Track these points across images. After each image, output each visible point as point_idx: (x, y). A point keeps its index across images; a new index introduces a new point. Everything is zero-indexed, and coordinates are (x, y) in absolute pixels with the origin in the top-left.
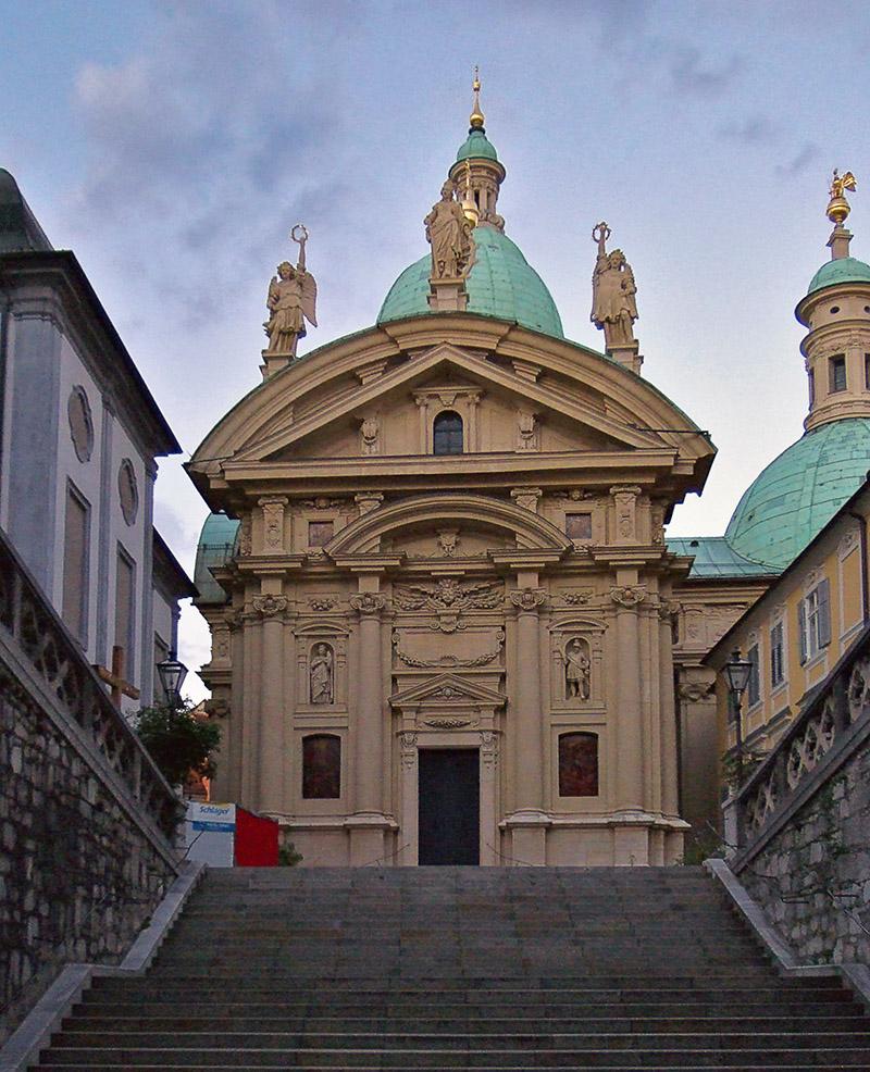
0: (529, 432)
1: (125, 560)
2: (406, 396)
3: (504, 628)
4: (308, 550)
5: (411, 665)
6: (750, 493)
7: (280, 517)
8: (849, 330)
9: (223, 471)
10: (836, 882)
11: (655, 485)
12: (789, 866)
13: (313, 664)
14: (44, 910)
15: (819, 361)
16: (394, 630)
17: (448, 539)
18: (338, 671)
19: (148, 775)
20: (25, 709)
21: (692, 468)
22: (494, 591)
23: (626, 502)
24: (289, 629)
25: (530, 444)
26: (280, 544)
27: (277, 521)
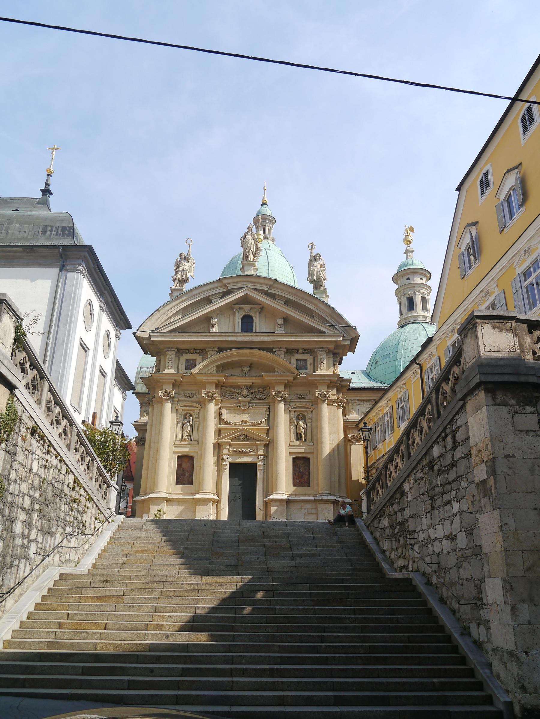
0: (281, 324)
1: (103, 374)
2: (231, 307)
3: (269, 408)
5: (227, 424)
6: (376, 353)
8: (414, 287)
9: (150, 337)
10: (408, 531)
12: (389, 523)
14: (40, 539)
15: (402, 298)
19: (100, 474)
20: (42, 442)
22: (265, 392)
23: (322, 355)
25: (282, 329)
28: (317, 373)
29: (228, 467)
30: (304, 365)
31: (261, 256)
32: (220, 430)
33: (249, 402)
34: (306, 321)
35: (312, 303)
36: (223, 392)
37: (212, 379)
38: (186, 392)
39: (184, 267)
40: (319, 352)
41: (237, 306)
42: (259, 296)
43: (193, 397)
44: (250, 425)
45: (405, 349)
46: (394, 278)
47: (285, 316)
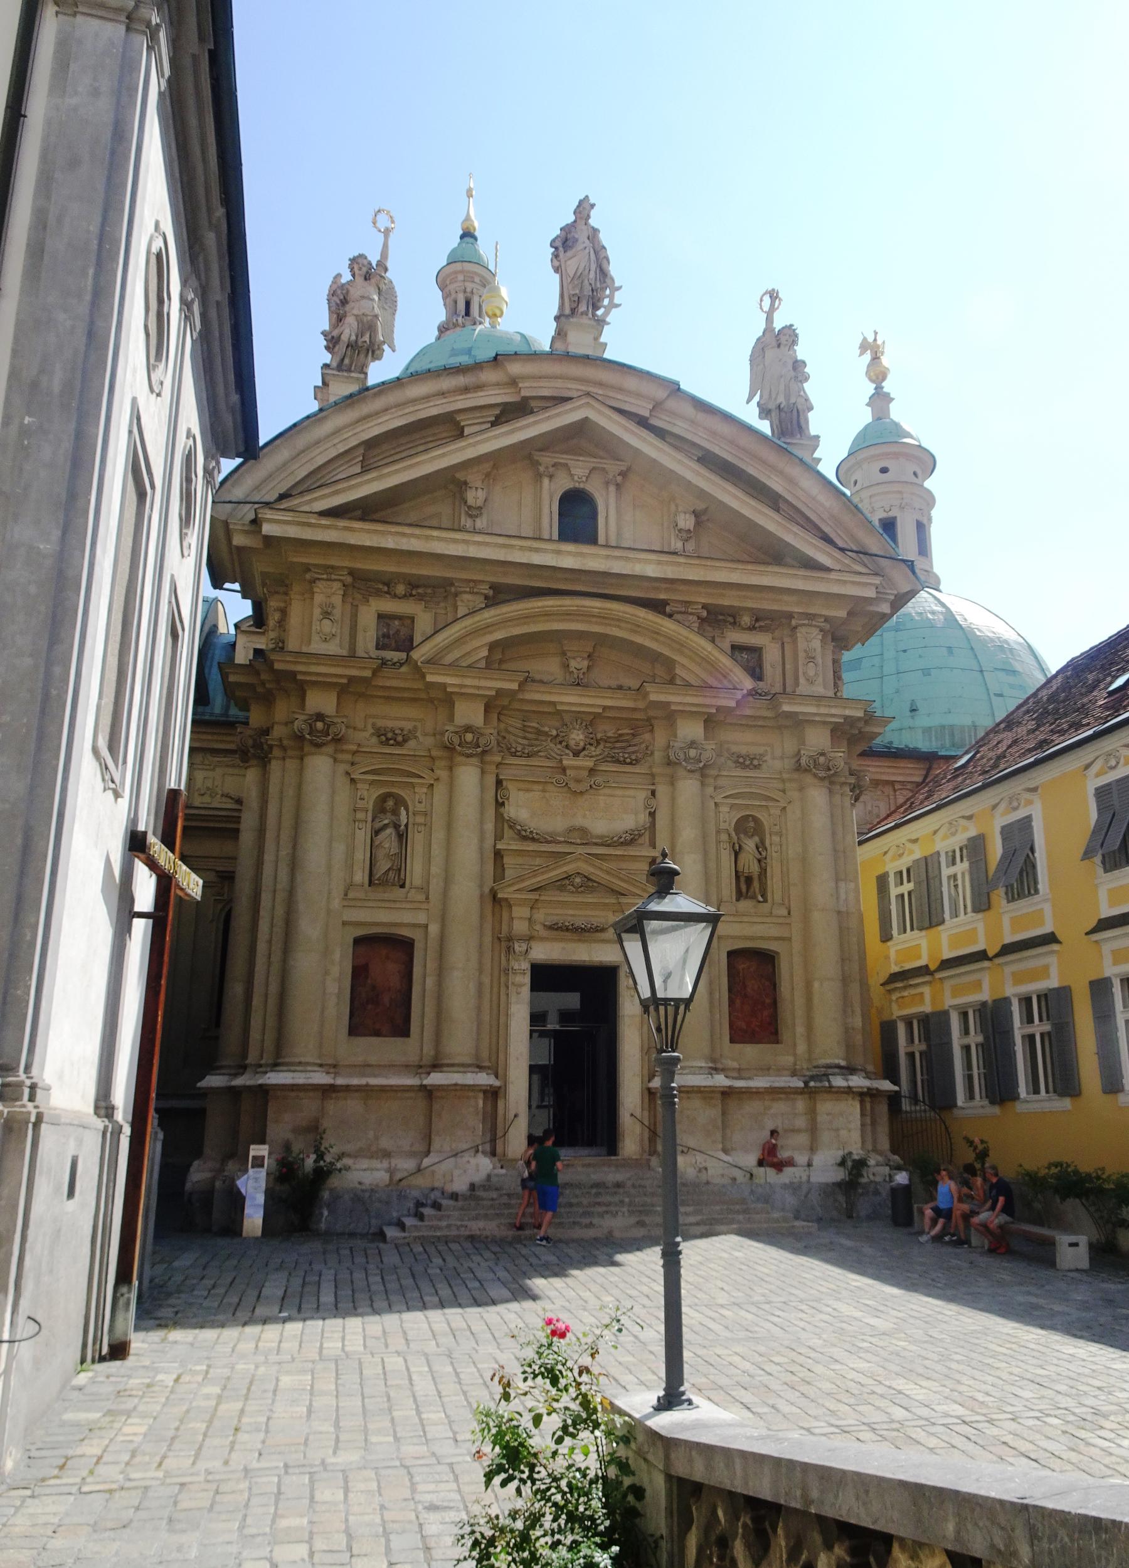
5: (525, 838)
7: (337, 600)
9: (256, 522)
13: (378, 825)
16: (499, 783)
18: (417, 839)
21: (888, 605)
22: (636, 740)
23: (811, 640)
24: (342, 768)
25: (690, 546)
26: (337, 640)
27: (333, 607)
29: (527, 979)
30: (751, 664)
31: (618, 306)
32: (498, 855)
33: (592, 771)
34: (771, 527)
35: (781, 473)
36: (506, 730)
37: (478, 688)
38: (380, 723)
40: (803, 630)
41: (546, 459)
42: (626, 429)
43: (405, 741)
44: (596, 844)
47: (701, 506)
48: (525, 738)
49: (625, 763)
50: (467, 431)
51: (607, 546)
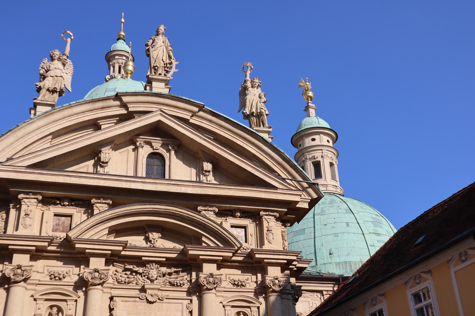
0: (209, 172)
4: (51, 234)
8: (322, 150)
11: (286, 213)
16: (111, 299)
17: (154, 236)
28: (265, 248)
38: (51, 269)
39: (58, 73)
43: (64, 278)
45: (325, 225)
46: (295, 138)
48: (126, 274)
49: (177, 286)
50: (103, 127)
51: (170, 180)
